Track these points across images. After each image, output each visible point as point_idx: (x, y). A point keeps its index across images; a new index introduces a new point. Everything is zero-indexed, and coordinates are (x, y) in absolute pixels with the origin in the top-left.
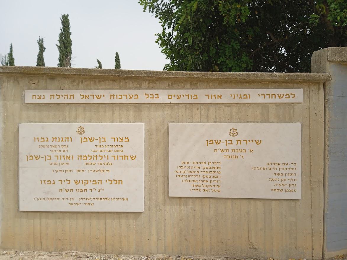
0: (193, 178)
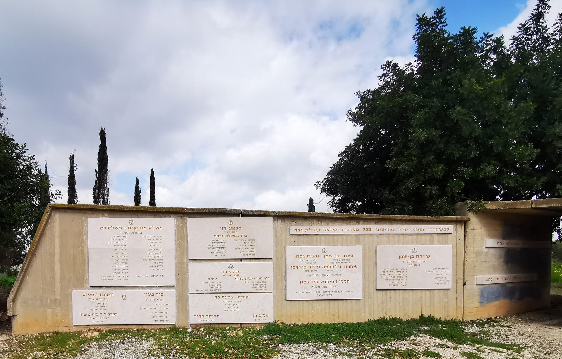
0: (391, 278)
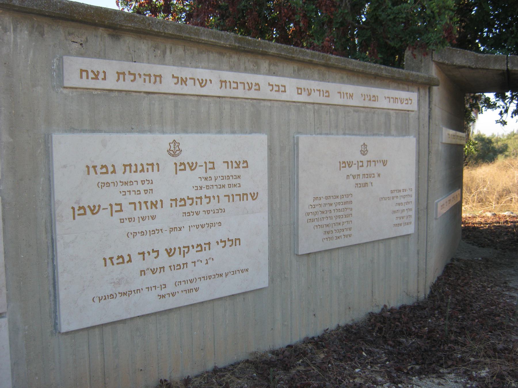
0: (325, 222)
